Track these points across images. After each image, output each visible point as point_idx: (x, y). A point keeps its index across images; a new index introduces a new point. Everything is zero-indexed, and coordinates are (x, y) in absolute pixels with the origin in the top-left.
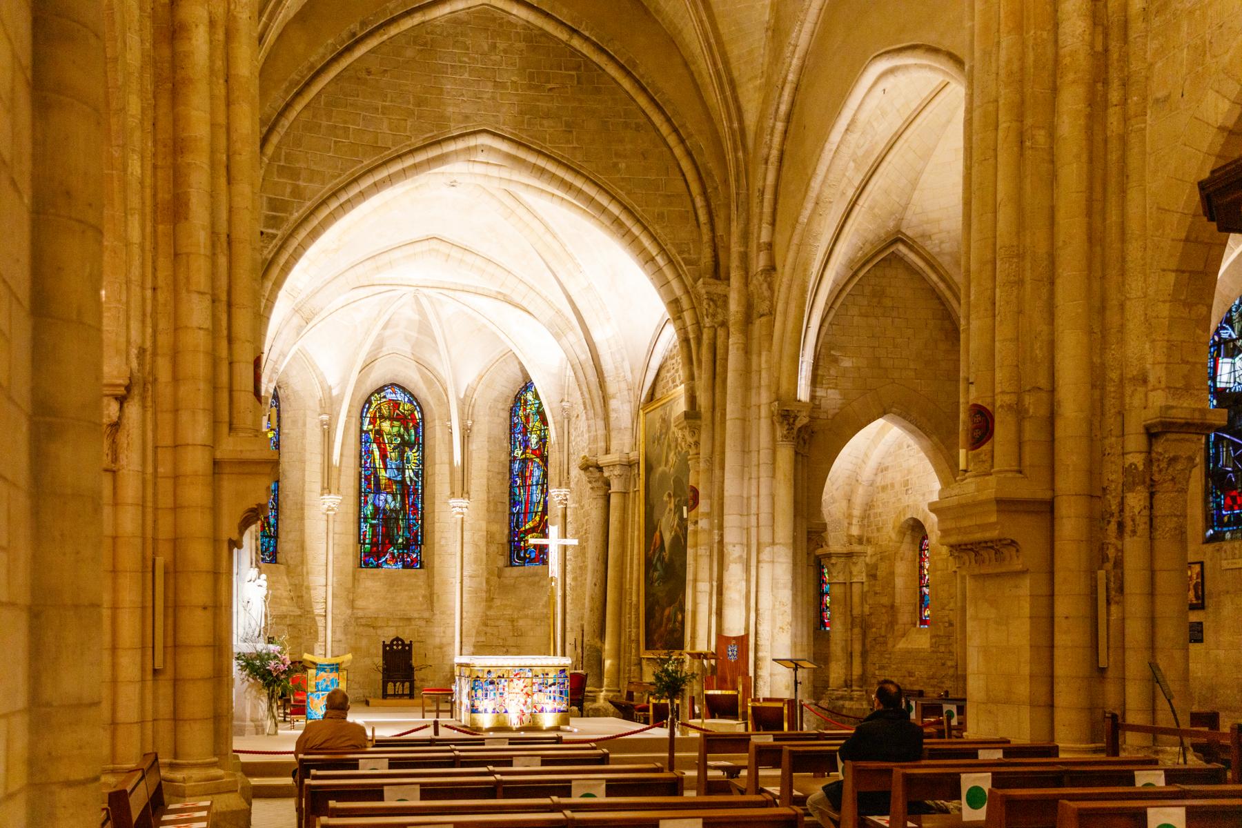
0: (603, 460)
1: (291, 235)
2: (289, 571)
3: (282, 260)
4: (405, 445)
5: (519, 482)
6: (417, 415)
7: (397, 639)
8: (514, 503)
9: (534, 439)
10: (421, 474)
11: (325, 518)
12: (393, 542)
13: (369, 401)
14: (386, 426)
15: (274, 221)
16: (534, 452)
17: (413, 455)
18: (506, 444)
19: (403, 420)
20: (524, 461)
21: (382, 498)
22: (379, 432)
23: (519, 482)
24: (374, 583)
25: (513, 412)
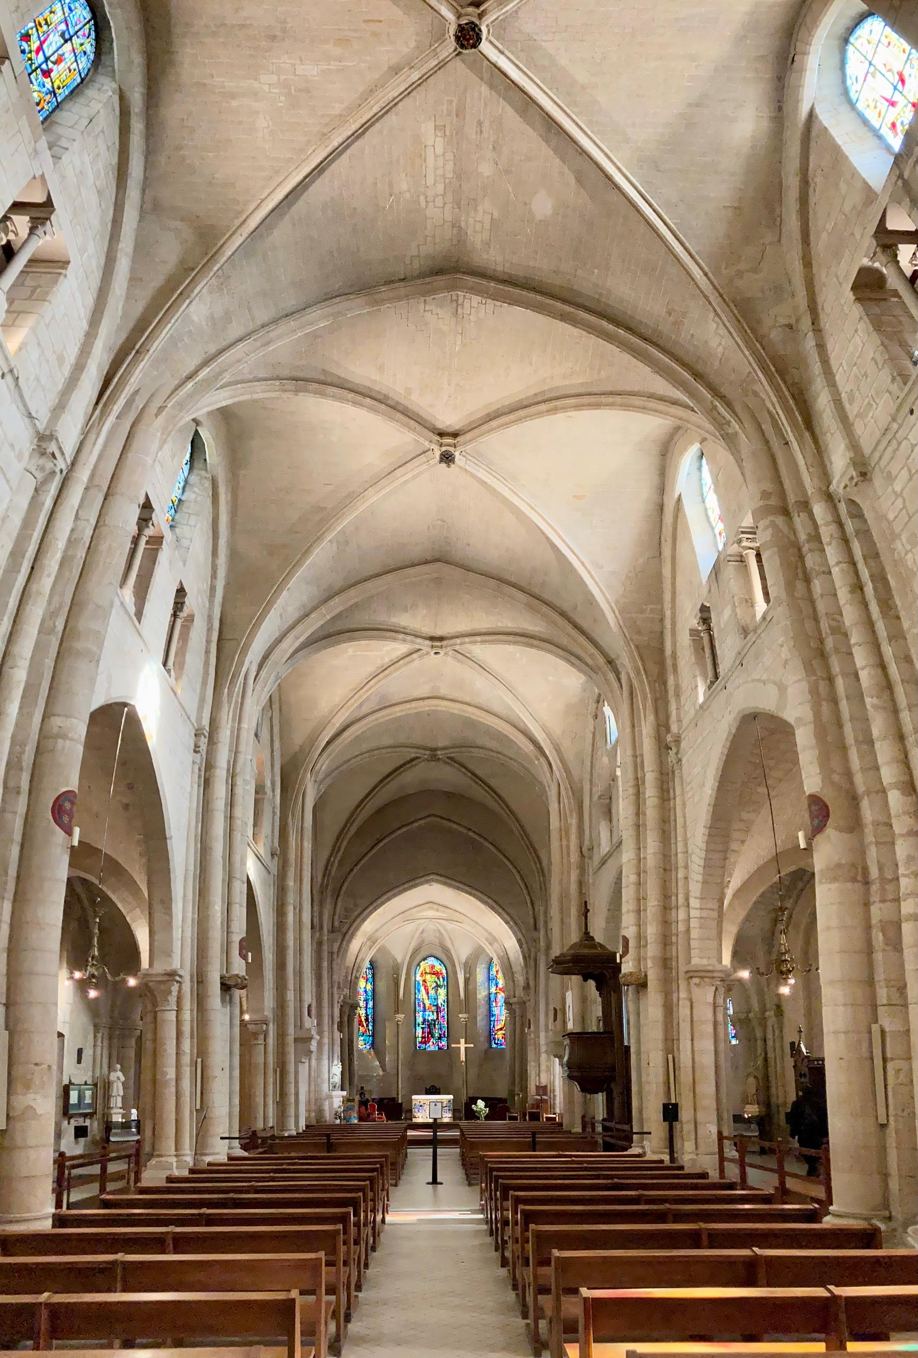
0: (512, 1000)
1: (354, 921)
3: (350, 932)
4: (438, 986)
5: (494, 1004)
7: (433, 1086)
13: (419, 965)
14: (428, 977)
15: (346, 917)
16: (500, 989)
19: (437, 974)
21: (427, 1013)
22: (424, 981)
23: (494, 1004)
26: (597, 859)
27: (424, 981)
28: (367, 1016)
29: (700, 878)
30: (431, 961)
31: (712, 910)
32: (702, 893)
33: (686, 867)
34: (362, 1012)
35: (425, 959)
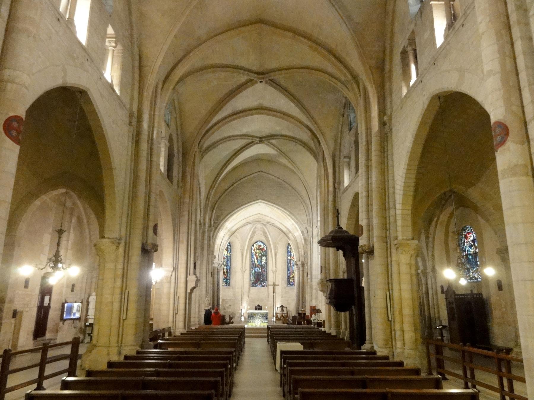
2: (232, 288)
4: (263, 256)
6: (265, 248)
8: (288, 270)
9: (292, 255)
10: (267, 263)
11: (241, 275)
12: (259, 280)
13: (253, 245)
14: (258, 251)
15: (217, 220)
17: (264, 258)
18: (286, 255)
19: (262, 250)
20: (291, 260)
24: (254, 290)
25: (288, 248)
26: (342, 189)
27: (256, 253)
28: (227, 269)
29: (401, 193)
30: (259, 243)
31: (409, 210)
32: (403, 201)
33: (394, 187)
34: (225, 267)
35: (256, 243)
